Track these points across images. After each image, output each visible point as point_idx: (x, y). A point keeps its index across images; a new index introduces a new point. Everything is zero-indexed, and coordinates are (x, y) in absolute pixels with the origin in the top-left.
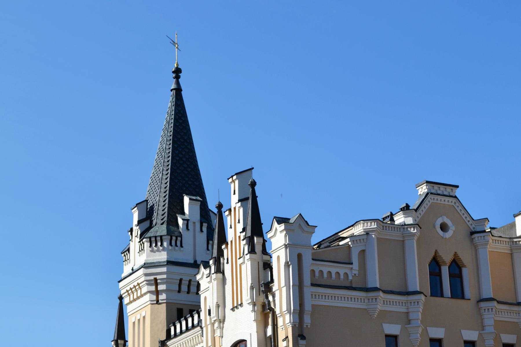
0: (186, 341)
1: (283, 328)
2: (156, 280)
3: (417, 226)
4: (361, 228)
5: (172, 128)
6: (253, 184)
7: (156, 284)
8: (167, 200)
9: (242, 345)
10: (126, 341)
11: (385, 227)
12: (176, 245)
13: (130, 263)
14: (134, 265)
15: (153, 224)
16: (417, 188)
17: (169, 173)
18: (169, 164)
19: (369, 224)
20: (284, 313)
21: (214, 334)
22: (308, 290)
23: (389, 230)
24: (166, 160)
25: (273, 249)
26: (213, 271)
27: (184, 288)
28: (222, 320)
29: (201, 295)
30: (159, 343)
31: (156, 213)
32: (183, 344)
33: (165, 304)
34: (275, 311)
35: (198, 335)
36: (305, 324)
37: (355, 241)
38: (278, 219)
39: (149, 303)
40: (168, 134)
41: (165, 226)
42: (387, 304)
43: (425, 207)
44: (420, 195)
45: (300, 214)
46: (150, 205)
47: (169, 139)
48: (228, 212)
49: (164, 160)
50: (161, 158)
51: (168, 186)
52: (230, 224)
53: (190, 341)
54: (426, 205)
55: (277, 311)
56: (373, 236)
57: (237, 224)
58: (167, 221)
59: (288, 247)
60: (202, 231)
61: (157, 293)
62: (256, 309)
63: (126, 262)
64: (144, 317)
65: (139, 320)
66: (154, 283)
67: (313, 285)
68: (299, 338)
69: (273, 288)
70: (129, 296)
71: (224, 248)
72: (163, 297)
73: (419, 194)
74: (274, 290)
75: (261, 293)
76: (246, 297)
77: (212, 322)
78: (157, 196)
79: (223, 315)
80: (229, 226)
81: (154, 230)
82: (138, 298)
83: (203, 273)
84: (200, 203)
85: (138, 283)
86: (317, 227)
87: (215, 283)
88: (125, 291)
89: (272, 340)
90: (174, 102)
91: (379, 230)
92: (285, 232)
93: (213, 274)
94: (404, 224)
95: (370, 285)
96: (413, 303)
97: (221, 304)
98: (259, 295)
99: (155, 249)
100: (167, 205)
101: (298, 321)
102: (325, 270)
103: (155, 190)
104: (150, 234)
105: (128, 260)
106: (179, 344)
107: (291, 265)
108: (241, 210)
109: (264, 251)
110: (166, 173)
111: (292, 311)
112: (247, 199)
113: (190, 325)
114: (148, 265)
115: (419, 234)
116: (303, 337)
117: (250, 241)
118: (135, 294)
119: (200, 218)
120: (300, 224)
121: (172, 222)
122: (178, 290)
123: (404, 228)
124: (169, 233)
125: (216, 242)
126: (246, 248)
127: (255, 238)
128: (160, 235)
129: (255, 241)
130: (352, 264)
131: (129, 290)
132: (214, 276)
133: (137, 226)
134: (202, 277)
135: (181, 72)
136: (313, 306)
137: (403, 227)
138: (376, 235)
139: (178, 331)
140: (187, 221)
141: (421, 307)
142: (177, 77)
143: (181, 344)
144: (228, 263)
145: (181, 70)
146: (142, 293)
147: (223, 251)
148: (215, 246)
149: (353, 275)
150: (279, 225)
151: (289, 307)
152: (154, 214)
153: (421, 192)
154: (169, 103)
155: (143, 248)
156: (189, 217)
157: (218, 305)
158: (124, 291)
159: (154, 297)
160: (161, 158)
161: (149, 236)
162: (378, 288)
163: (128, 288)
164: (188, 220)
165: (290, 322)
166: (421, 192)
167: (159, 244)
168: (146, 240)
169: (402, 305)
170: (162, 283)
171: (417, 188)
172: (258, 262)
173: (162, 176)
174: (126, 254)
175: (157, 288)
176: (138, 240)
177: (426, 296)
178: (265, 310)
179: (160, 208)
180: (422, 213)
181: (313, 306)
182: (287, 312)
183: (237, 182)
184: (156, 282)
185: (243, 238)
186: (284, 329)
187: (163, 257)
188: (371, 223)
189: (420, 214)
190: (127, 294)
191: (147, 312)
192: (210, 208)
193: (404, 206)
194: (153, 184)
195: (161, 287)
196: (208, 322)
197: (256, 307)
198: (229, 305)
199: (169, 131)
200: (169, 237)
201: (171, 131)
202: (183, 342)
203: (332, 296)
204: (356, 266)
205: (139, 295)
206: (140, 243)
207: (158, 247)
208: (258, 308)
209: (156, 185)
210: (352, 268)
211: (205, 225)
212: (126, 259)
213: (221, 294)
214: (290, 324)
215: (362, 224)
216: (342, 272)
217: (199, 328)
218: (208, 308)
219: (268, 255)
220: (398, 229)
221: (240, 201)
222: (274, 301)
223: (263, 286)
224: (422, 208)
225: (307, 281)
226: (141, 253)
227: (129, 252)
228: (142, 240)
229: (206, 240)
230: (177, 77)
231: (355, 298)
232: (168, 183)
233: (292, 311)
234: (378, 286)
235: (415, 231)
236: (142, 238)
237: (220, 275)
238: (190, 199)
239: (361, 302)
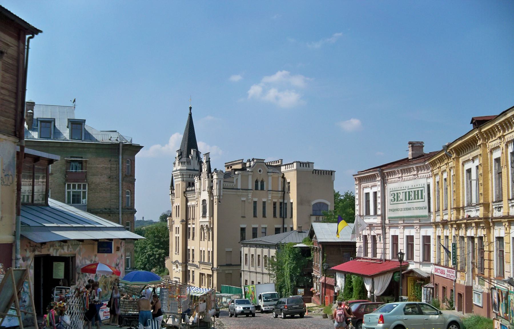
6: (209, 159)
27: (191, 177)
55: (214, 195)
67: (223, 188)
76: (206, 189)
82: (178, 178)
95: (239, 188)
102: (227, 184)
116: (220, 202)
121: (188, 157)
132: (198, 181)
136: (223, 194)
140: (192, 157)
142: (190, 110)
176: (178, 161)
191: (180, 182)
192: (199, 150)
198: (202, 189)
204: (235, 183)
208: (209, 192)
211: (197, 158)
216: (231, 185)
225: (222, 188)
230: (190, 110)
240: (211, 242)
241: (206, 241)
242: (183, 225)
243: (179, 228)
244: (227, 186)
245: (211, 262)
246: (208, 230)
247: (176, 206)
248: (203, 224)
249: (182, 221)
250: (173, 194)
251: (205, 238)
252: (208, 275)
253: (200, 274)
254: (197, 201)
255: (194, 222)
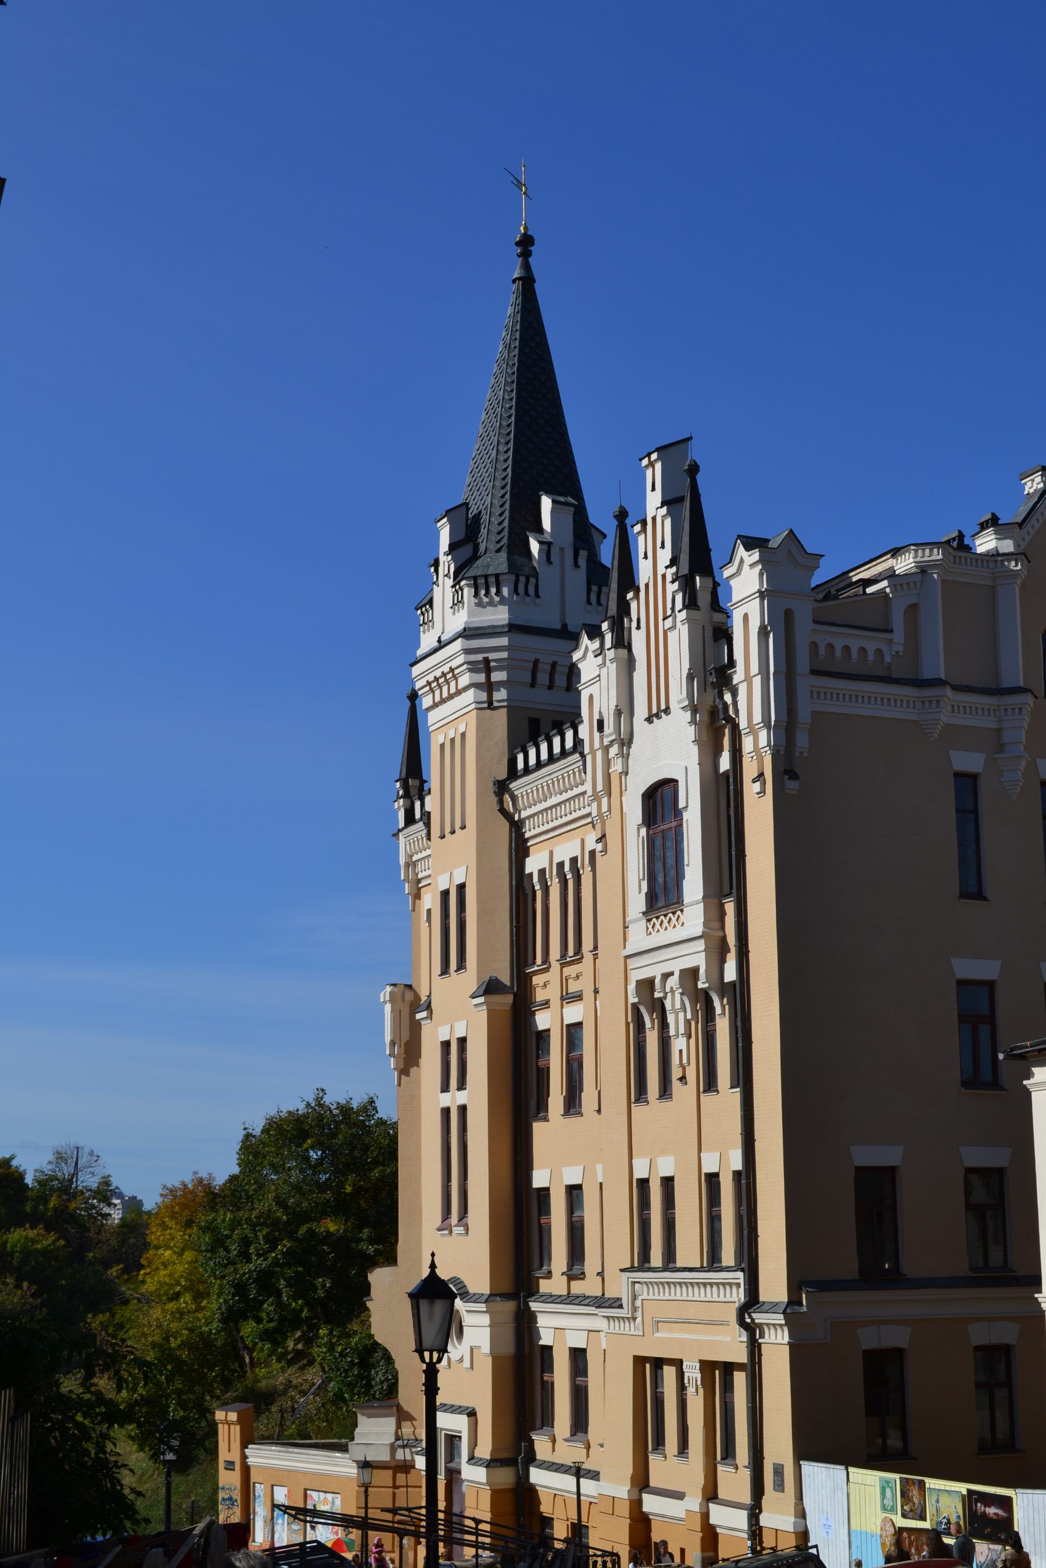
0: (549, 782)
1: (752, 757)
2: (487, 661)
3: (1023, 557)
4: (911, 560)
5: (516, 358)
6: (693, 470)
7: (488, 671)
8: (508, 503)
9: (667, 789)
10: (423, 782)
11: (957, 559)
12: (527, 593)
13: (433, 628)
14: (442, 633)
15: (480, 551)
16: (1023, 482)
17: (512, 449)
18: (511, 431)
19: (927, 551)
20: (757, 727)
21: (609, 768)
22: (805, 683)
23: (966, 565)
24: (505, 423)
25: (734, 600)
26: (608, 643)
27: (543, 678)
28: (626, 741)
29: (582, 691)
30: (495, 784)
31: (486, 529)
32: (543, 787)
33: (505, 710)
34: (737, 722)
35: (573, 770)
36: (797, 749)
37: (899, 587)
38: (745, 540)
39: (473, 706)
40: (508, 370)
41: (503, 556)
42: (959, 712)
43: (1038, 520)
44: (1028, 494)
45: (791, 531)
46: (473, 514)
47: (509, 380)
48: (639, 525)
49: (500, 424)
50: (494, 419)
51: (510, 475)
52: (644, 550)
53: (558, 781)
54: (1040, 516)
55: (743, 724)
56: (935, 576)
57: (659, 550)
58: (508, 546)
59: (766, 596)
60: (576, 565)
61: (489, 687)
62: (698, 719)
63: (426, 626)
64: (463, 735)
65: (453, 740)
66: (484, 669)
67: (814, 672)
68: (785, 776)
69: (732, 678)
70: (432, 694)
71: (631, 599)
72: (500, 695)
73: (1026, 493)
74: (735, 682)
75: (709, 689)
76: (678, 693)
77: (605, 743)
78: (487, 495)
79: (629, 730)
80: (641, 555)
81: (482, 563)
82: (451, 697)
83: (587, 647)
84: (572, 509)
85: (451, 668)
86: (823, 556)
87: (613, 667)
88: (425, 683)
89: (731, 780)
90: (519, 304)
91: (946, 564)
92: (760, 567)
93: (609, 649)
94: (995, 553)
95: (927, 674)
96: (1010, 711)
97: (625, 709)
98: (705, 691)
99: (486, 600)
100: (507, 514)
101: (784, 743)
102: (839, 644)
103: (483, 483)
104: (475, 571)
105: (430, 621)
106: (535, 788)
107: (772, 633)
108: (668, 522)
109: (716, 605)
110: (505, 449)
111: (773, 723)
112: (680, 500)
113: (557, 749)
114: (472, 633)
115: (1026, 573)
116: (793, 775)
117: (686, 584)
118: (445, 689)
119: (574, 541)
120: (789, 551)
122: (530, 681)
123: (996, 561)
124: (514, 568)
125: (614, 585)
126: (679, 598)
127: (698, 578)
128: (495, 572)
129: (698, 585)
130: (892, 631)
131: (433, 682)
132: (610, 654)
133: (448, 555)
134: (584, 656)
135: (533, 244)
136: (814, 714)
137: (995, 558)
138: (942, 575)
139: (532, 761)
141: (1026, 717)
142: (526, 255)
143: (539, 786)
144: (638, 627)
145: (534, 240)
146: (460, 687)
147: (629, 604)
148: (614, 596)
149: (894, 653)
150: (748, 551)
151: (766, 715)
152: (482, 530)
153: (1030, 488)
154: (510, 307)
155: (460, 599)
156: (552, 537)
157: (619, 710)
158: (423, 682)
159: (484, 696)
160: (494, 419)
161: (473, 575)
162: (943, 680)
163: (431, 678)
164: (549, 544)
165: (769, 745)
166: (1030, 488)
167: (493, 590)
168: (468, 582)
169: (989, 715)
170: (497, 669)
171: (1022, 480)
172: (704, 626)
173: (497, 455)
174: (426, 610)
175: (488, 677)
176: (450, 582)
177: (1036, 698)
178: (715, 722)
179: (493, 519)
180: (1033, 532)
181: (814, 714)
182: (762, 725)
183: (658, 466)
184: (487, 667)
185: (671, 580)
186: (755, 758)
187: (501, 617)
188: (931, 550)
189: (1028, 533)
190: (427, 688)
191: (469, 725)
193: (987, 518)
194: (478, 470)
195: (498, 676)
196: (597, 745)
197: (698, 715)
198: (641, 710)
199: (511, 363)
200: (513, 577)
201: (514, 365)
202: (542, 784)
203: (850, 696)
204: (899, 634)
205: (453, 690)
206: (454, 590)
207: (492, 597)
209: (484, 474)
210: (891, 640)
211: (583, 554)
212: (426, 621)
213: (625, 690)
214: (768, 748)
215: (913, 552)
216: (871, 647)
217: (576, 756)
218: (596, 717)
219: (723, 612)
220: (985, 562)
221: (663, 504)
222: (735, 703)
223: (714, 674)
224: (1033, 521)
225: (803, 664)
226: (456, 608)
227: (431, 607)
228: (459, 583)
229: (585, 583)
230: (526, 255)
231: (895, 700)
232: (509, 470)
233: (773, 723)
234: (943, 677)
235: (1019, 567)
236: (458, 579)
237: (624, 652)
238: (554, 502)
239: (908, 707)
240: (729, 1097)
241: (684, 1094)
242: (490, 1013)
243: (462, 1041)
244: (838, 653)
245: (728, 1255)
246: (703, 1002)
247: (445, 894)
248: (655, 972)
249: (491, 988)
250: (420, 825)
251: (676, 1073)
252: (707, 1367)
253: (640, 1362)
254: (597, 822)
255: (573, 987)
